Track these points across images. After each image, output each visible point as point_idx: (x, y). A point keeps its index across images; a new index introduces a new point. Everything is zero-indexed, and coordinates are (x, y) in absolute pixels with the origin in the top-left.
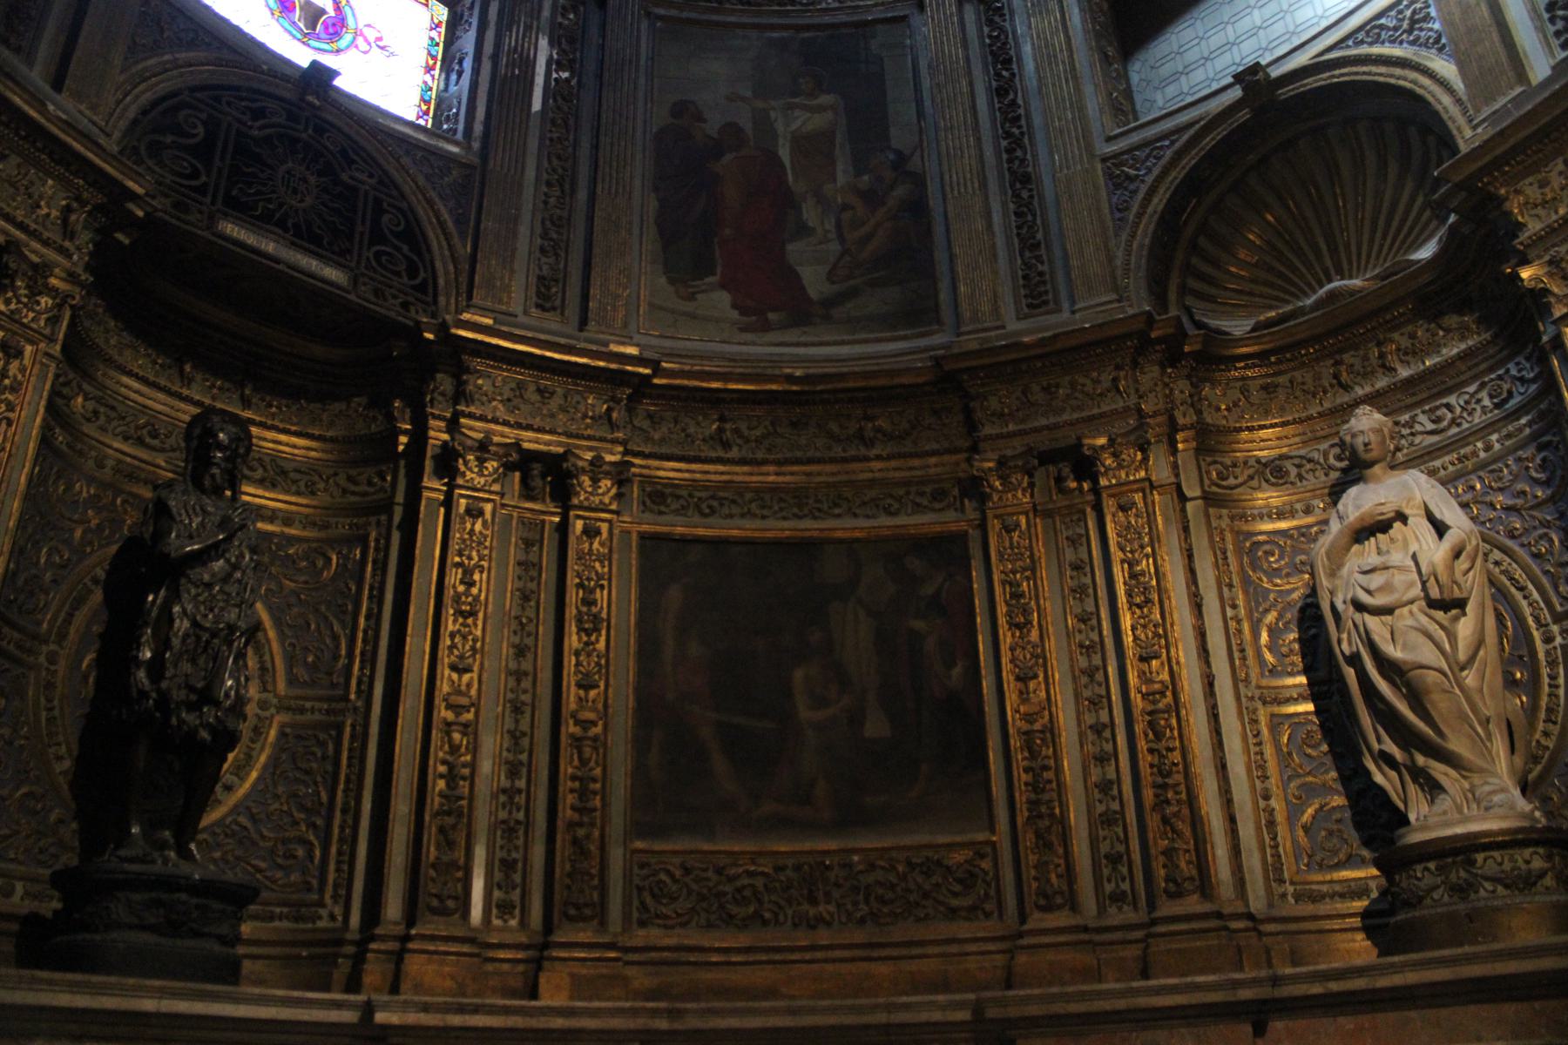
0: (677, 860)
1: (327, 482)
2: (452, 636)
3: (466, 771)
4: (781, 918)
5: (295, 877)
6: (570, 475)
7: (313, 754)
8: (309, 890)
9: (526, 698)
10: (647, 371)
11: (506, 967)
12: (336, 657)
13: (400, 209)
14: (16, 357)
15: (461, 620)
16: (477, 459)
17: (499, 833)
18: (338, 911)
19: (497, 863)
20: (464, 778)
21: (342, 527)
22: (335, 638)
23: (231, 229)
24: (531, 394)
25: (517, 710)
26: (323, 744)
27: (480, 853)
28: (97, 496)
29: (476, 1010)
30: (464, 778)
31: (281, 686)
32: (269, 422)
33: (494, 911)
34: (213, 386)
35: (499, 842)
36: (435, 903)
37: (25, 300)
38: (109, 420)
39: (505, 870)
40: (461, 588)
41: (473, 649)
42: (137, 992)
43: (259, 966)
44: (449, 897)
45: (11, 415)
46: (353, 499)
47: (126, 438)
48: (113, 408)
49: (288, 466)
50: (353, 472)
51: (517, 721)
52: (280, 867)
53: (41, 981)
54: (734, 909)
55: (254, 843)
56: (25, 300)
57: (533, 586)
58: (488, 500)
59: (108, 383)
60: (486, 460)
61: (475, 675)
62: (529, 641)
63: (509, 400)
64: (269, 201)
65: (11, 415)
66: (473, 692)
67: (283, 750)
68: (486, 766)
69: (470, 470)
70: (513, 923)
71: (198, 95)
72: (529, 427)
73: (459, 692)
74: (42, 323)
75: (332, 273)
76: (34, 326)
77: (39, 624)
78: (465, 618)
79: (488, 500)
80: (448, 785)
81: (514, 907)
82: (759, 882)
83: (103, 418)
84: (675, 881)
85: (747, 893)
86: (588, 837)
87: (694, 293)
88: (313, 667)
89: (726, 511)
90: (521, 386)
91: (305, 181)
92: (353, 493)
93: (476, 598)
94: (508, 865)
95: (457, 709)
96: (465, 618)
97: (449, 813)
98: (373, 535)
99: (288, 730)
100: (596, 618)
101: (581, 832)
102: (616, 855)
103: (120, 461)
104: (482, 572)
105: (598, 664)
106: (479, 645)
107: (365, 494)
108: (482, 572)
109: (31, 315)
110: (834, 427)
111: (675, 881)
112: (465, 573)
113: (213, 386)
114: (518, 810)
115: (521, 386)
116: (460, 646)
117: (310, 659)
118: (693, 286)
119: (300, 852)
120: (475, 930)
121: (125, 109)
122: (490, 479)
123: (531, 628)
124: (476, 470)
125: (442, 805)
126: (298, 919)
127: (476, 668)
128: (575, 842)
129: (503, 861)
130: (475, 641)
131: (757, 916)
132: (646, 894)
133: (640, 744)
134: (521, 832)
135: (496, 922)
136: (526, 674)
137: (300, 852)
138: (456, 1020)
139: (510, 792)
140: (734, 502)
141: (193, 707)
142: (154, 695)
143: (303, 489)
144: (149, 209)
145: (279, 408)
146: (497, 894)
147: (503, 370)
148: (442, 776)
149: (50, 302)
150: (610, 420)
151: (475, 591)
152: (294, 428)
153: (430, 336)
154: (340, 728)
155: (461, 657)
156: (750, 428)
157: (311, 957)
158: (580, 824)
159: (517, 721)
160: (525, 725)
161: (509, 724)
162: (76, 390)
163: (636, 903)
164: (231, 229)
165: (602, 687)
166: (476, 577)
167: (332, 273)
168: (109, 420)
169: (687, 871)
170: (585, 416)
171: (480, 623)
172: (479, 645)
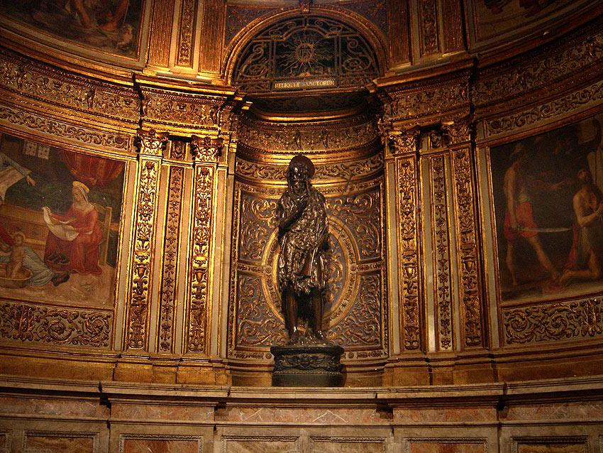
0: (523, 309)
1: (364, 166)
2: (403, 225)
3: (416, 284)
4: (576, 333)
5: (373, 338)
6: (446, 131)
7: (373, 285)
8: (378, 343)
9: (445, 243)
10: (471, 65)
11: (444, 369)
12: (376, 242)
13: (357, 38)
14: (206, 175)
15: (405, 216)
16: (403, 139)
17: (439, 308)
18: (386, 350)
19: (439, 322)
20: (415, 288)
21: (371, 184)
22: (375, 234)
23: (279, 86)
24: (424, 98)
25: (442, 250)
26: (375, 281)
27: (430, 320)
28: (273, 205)
29: (419, 391)
30: (415, 288)
31: (360, 260)
32: (336, 149)
33: (441, 344)
34: (311, 143)
35: (439, 312)
36: (408, 344)
37: (205, 153)
38: (272, 174)
39: (444, 325)
40: (404, 202)
41: (413, 228)
42: (287, 392)
43: (355, 376)
44: (414, 341)
45: (210, 196)
46: (375, 170)
47: (280, 179)
48: (273, 169)
49: (347, 165)
50: (372, 159)
51: (443, 255)
52: (367, 334)
53: (250, 390)
54: (553, 330)
55: (357, 326)
56: (205, 153)
57: (443, 189)
58: (411, 157)
59: (269, 160)
60: (407, 139)
61: (415, 239)
62: (444, 216)
63: (414, 105)
64: (295, 65)
65: (210, 196)
66: (415, 248)
67: (362, 286)
68: (429, 279)
69: (401, 146)
70: (450, 348)
71: (259, 37)
72: (423, 115)
73: (407, 250)
74: (213, 158)
75: (325, 83)
76: (210, 161)
77: (260, 260)
78: (407, 215)
79: (411, 157)
80: (408, 292)
81: (450, 342)
82: (564, 314)
83: (270, 174)
84: (524, 319)
85: (558, 321)
86: (473, 305)
87: (501, 8)
88: (368, 249)
89: (530, 119)
90: (419, 97)
91: (309, 48)
92: (373, 168)
93: (412, 205)
94: (445, 322)
95: (408, 257)
96: (407, 215)
97: (409, 304)
98: (381, 184)
99: (363, 277)
100: (468, 197)
101: (469, 303)
102: (493, 312)
103: (279, 189)
104: (412, 191)
105: (470, 220)
106: (415, 226)
107: (376, 167)
108: (412, 191)
109: (208, 157)
110: (575, 52)
111: (524, 319)
112: (405, 194)
113: (311, 143)
114: (447, 296)
115: (419, 97)
116: (407, 228)
117: (367, 246)
118: (500, 4)
119: (374, 328)
120: (431, 354)
121: (232, 59)
122: (410, 147)
123: (444, 208)
124: (403, 145)
125: (406, 301)
126: (376, 355)
127: (415, 237)
128: (468, 308)
129: (442, 321)
130: (413, 224)
131: (563, 332)
132: (510, 328)
133: (502, 254)
134: (449, 307)
135: (442, 349)
136: (444, 232)
137: (374, 328)
138: (412, 395)
139: (443, 289)
140: (533, 113)
141: (300, 281)
142: (286, 280)
143: (356, 172)
144: (243, 96)
145: (340, 141)
146: (441, 336)
147: (409, 92)
148: (405, 289)
149: (214, 149)
150: (461, 96)
151: (410, 201)
152: (346, 148)
153: (372, 91)
154: (379, 272)
155: (408, 233)
156: (535, 70)
157: (378, 370)
158: (469, 299)
159: (443, 255)
160: (446, 257)
161: (438, 257)
162: (255, 168)
163: (505, 333)
164: (279, 86)
165: (474, 231)
166: (410, 194)
167: (325, 83)
168: (272, 174)
169: (529, 314)
170: (450, 98)
171: (414, 215)
172: (415, 226)
